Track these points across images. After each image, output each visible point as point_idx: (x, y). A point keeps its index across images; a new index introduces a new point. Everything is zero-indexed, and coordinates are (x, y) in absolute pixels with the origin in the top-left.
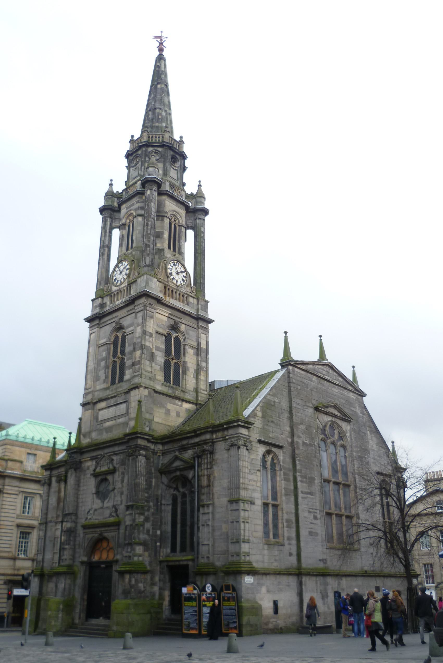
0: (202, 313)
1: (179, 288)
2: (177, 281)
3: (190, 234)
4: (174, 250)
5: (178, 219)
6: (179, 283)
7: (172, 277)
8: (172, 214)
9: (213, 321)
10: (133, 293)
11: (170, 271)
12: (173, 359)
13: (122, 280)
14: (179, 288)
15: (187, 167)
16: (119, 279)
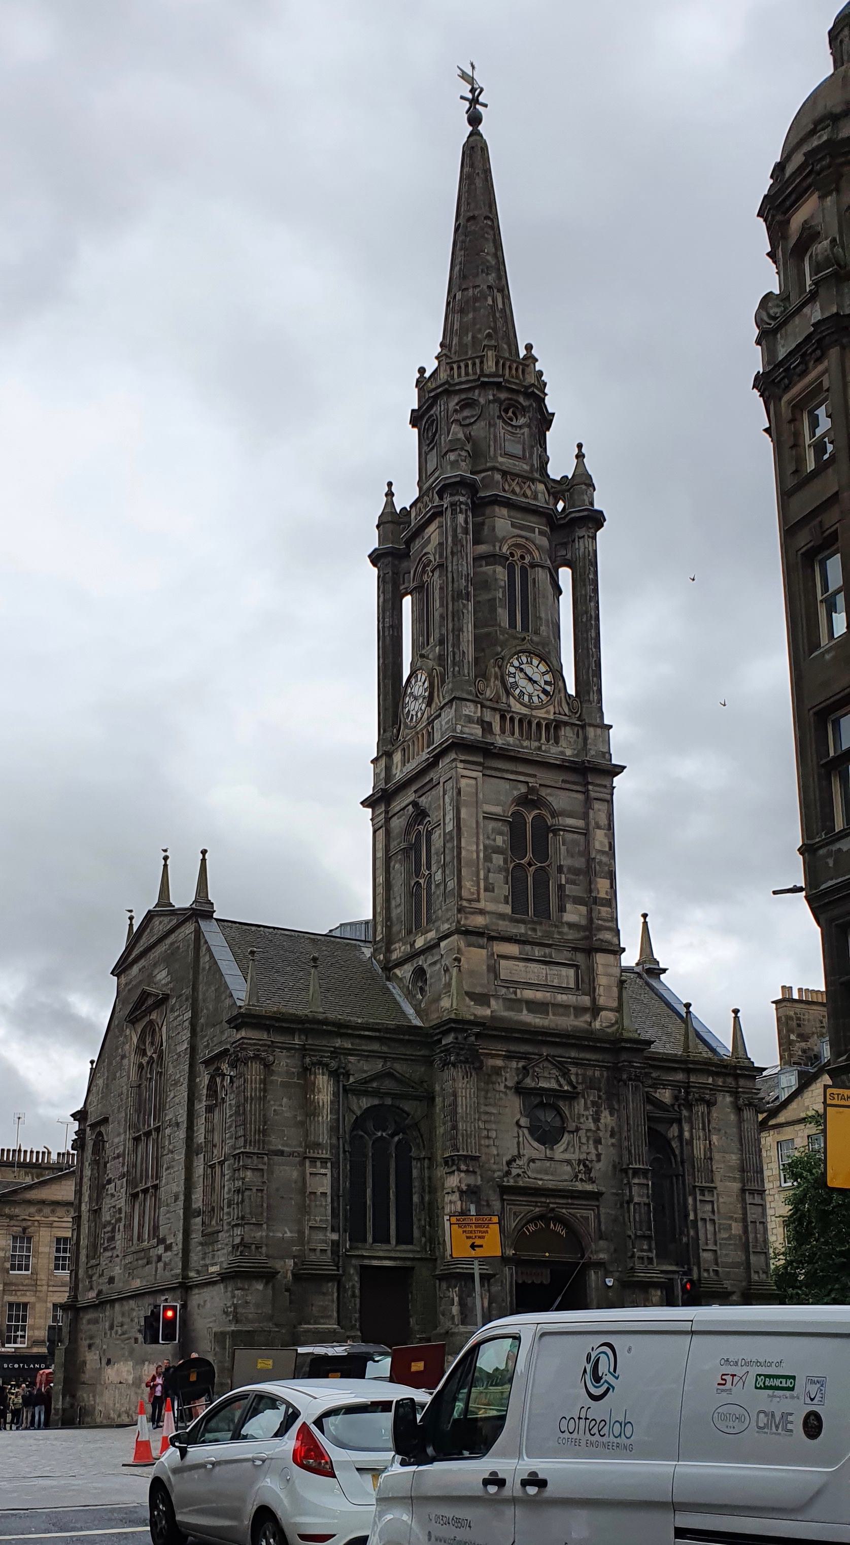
0: (592, 755)
1: (535, 713)
2: (530, 696)
3: (565, 575)
4: (525, 628)
5: (531, 553)
6: (535, 699)
7: (518, 691)
8: (513, 545)
9: (624, 767)
10: (438, 739)
11: (512, 680)
12: (530, 865)
13: (419, 715)
14: (535, 713)
15: (553, 414)
16: (414, 713)
